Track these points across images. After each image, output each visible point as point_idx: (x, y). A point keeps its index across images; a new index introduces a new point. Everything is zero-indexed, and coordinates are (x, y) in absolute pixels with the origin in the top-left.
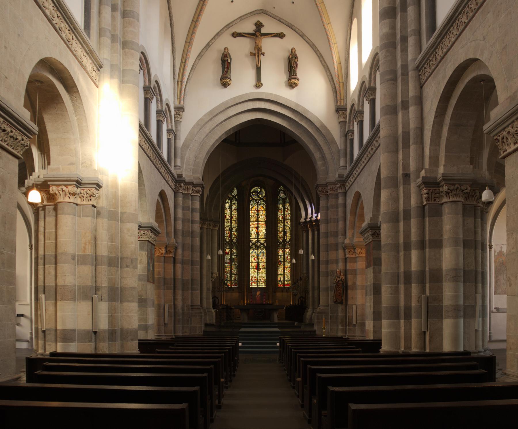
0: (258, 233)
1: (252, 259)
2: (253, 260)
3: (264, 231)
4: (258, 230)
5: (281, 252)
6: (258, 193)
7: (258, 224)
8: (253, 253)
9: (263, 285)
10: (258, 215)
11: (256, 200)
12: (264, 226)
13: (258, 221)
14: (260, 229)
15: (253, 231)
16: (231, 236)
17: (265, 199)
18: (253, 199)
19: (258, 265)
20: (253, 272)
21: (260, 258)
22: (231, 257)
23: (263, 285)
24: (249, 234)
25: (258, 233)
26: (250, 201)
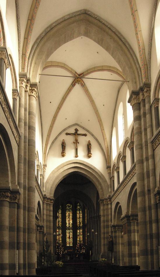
0: (69, 223)
1: (67, 234)
2: (68, 235)
3: (72, 222)
4: (69, 222)
5: (78, 231)
6: (69, 207)
7: (69, 219)
8: (67, 231)
9: (71, 245)
10: (69, 215)
11: (68, 209)
12: (71, 220)
13: (69, 218)
14: (70, 221)
15: (67, 222)
16: (59, 224)
17: (72, 209)
18: (67, 209)
19: (69, 236)
20: (68, 240)
21: (70, 233)
22: (59, 233)
23: (71, 245)
24: (66, 224)
25: (69, 223)
26: (66, 210)
